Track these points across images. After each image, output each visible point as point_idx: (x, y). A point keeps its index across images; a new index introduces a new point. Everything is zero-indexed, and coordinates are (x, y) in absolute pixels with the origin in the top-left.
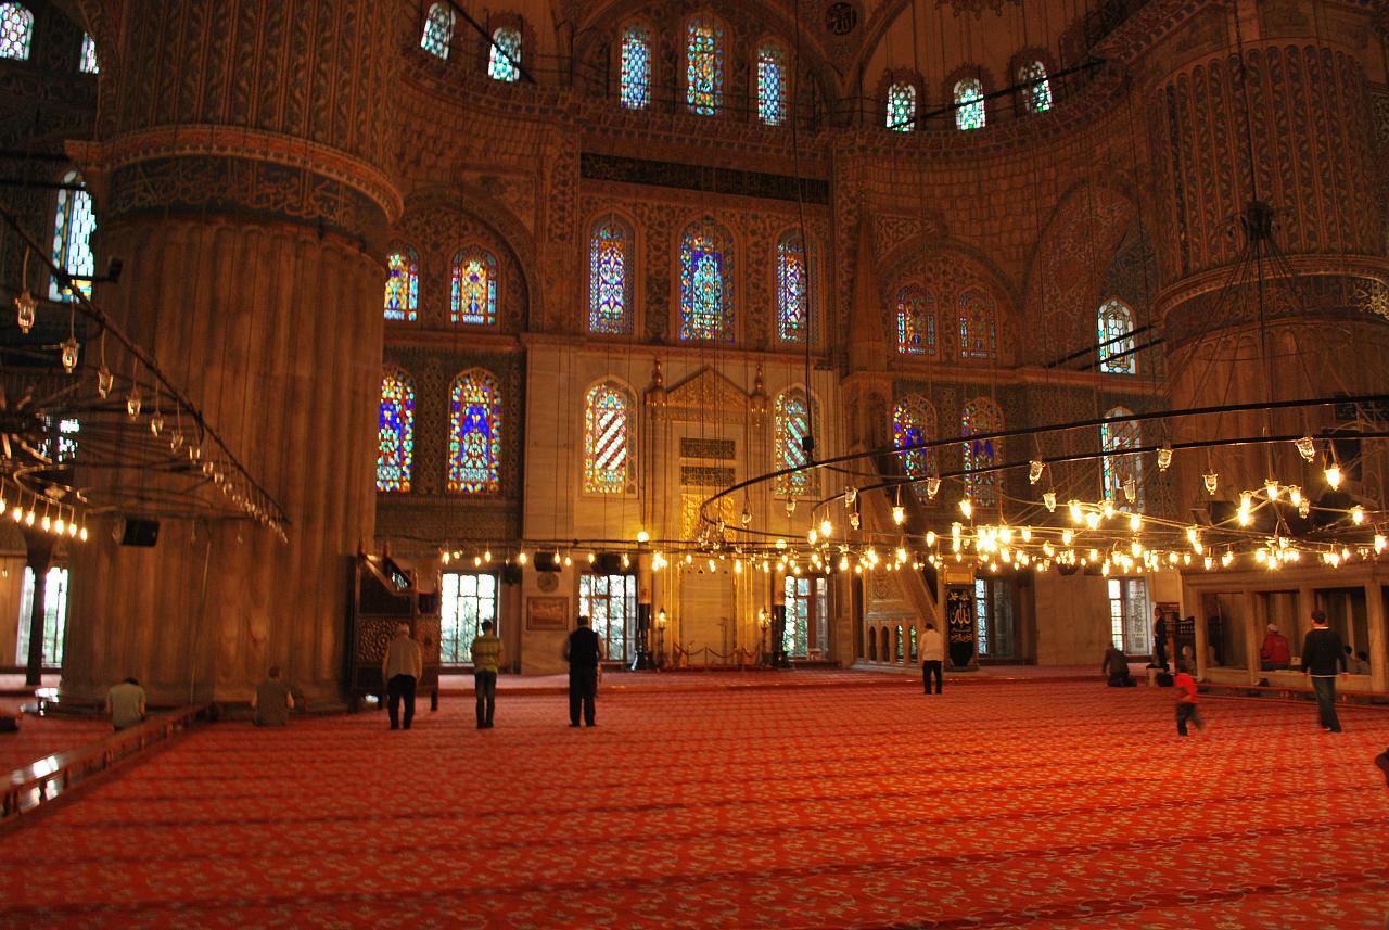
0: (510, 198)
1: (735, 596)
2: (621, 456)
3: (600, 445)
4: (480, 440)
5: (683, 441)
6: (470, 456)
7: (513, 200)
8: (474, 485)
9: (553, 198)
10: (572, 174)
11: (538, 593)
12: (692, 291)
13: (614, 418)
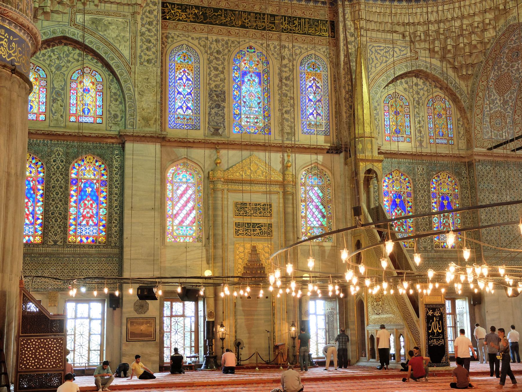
0: (112, 34)
1: (274, 314)
2: (193, 215)
3: (177, 208)
5: (236, 204)
6: (84, 217)
7: (114, 35)
8: (87, 238)
9: (142, 34)
10: (156, 17)
13: (186, 190)
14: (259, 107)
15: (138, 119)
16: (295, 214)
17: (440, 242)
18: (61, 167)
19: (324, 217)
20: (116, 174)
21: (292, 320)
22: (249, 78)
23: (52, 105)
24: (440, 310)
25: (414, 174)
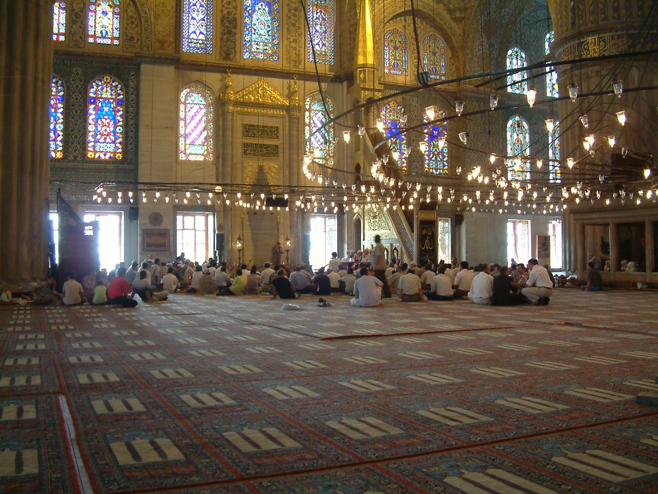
1: (278, 229)
4: (109, 124)
5: (245, 126)
6: (102, 135)
8: (105, 155)
11: (149, 226)
12: (251, 27)
14: (269, 35)
15: (153, 41)
18: (80, 86)
20: (132, 94)
22: (260, 7)
23: (72, 27)
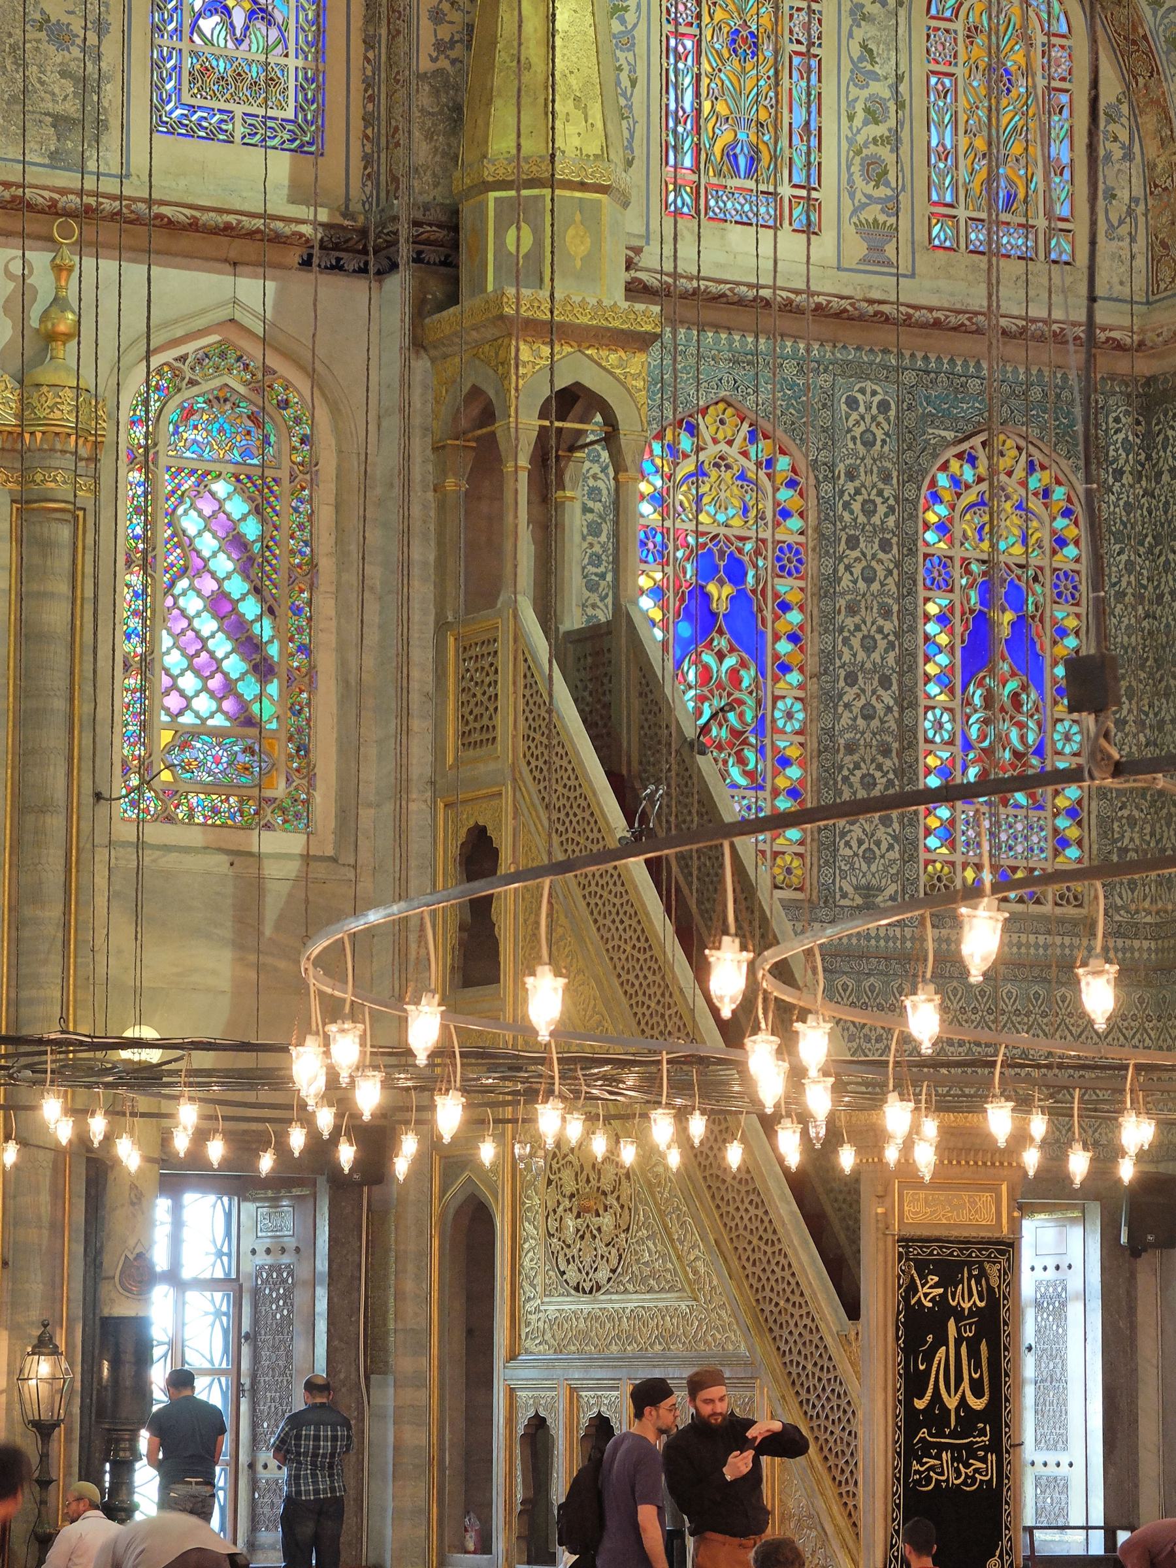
16: (84, 643)
17: (958, 858)
19: (262, 669)
21: (35, 1315)
24: (983, 1273)
25: (830, 434)
